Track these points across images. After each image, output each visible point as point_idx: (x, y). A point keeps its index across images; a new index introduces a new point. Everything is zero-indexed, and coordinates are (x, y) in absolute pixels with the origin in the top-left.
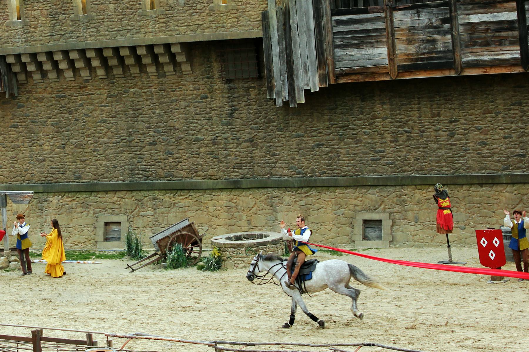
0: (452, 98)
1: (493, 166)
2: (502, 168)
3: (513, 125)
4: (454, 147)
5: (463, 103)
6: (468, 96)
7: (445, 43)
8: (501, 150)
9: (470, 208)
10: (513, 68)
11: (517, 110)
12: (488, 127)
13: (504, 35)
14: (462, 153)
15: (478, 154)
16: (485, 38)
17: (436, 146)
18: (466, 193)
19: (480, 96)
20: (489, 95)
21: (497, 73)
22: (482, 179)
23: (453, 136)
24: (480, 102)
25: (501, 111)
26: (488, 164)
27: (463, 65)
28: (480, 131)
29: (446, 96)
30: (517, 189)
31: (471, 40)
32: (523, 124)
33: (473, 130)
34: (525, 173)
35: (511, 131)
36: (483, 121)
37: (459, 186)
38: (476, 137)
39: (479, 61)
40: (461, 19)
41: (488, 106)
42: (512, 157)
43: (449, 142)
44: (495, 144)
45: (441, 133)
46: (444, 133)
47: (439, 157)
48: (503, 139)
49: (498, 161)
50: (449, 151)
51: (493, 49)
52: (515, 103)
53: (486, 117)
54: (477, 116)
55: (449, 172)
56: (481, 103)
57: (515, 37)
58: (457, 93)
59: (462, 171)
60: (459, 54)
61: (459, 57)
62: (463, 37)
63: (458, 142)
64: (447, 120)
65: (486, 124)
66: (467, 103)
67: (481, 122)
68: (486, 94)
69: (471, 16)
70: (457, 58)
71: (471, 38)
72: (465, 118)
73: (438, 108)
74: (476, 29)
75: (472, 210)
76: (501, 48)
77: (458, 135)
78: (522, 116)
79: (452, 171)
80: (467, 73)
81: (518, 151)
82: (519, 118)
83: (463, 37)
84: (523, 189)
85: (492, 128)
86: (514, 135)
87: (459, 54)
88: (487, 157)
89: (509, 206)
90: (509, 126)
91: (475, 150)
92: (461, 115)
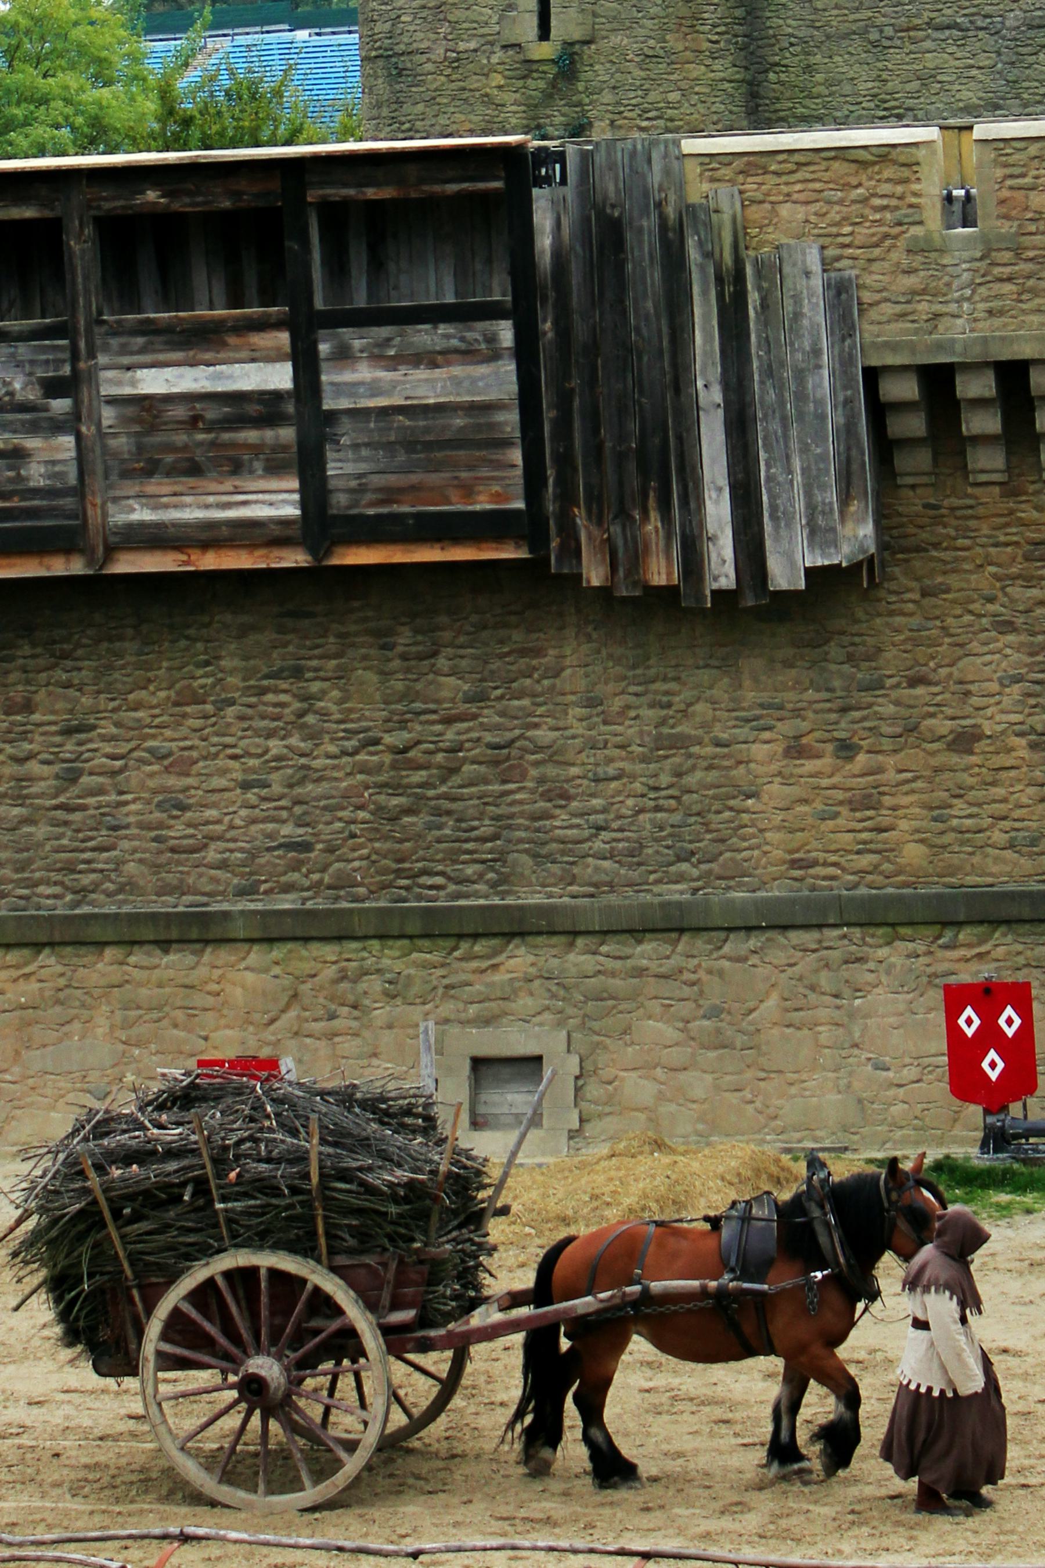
0: (75, 649)
1: (204, 880)
2: (236, 886)
3: (272, 743)
4: (77, 817)
5: (110, 667)
6: (127, 644)
7: (54, 463)
8: (232, 827)
9: (127, 1025)
10: (276, 552)
11: (285, 691)
12: (190, 748)
13: (250, 441)
14: (102, 837)
15: (155, 839)
16: (185, 448)
17: (16, 811)
18: (115, 974)
19: (166, 644)
20: (194, 640)
21: (224, 567)
22: (168, 927)
23: (74, 781)
24: (165, 664)
25: (237, 695)
26: (188, 873)
27: (112, 539)
28: (166, 762)
29: (54, 642)
30: (283, 960)
31: (139, 454)
32: (303, 740)
33: (140, 760)
34: (309, 905)
35: (268, 761)
36: (174, 730)
37: (92, 949)
38: (151, 783)
39: (166, 527)
40: (110, 381)
41: (193, 678)
42: (269, 849)
43: (62, 799)
44: (215, 805)
45: (34, 767)
46: (45, 767)
47: (27, 850)
48: (239, 791)
49: (223, 865)
50: (61, 830)
51: (213, 487)
52: (282, 670)
53: (185, 716)
54: (157, 711)
55: (59, 902)
56: (169, 669)
57: (284, 448)
58: (89, 632)
59: (102, 897)
60: (99, 501)
61: (99, 511)
62: (113, 443)
63: (91, 801)
64: (55, 723)
65: (185, 739)
66: (123, 667)
67: (168, 733)
68: (187, 638)
69: (141, 373)
70: (93, 515)
71: (140, 448)
72: (115, 716)
73: (28, 682)
74: (156, 417)
75: (135, 1031)
76: (237, 483)
77: (91, 774)
78: (301, 714)
79: (69, 897)
80: (127, 564)
81: (287, 830)
82: (292, 718)
83: (113, 443)
84: (301, 959)
85: (204, 753)
86: (275, 776)
87: (99, 501)
88: (184, 852)
89: (256, 1017)
90: (258, 746)
91: (150, 829)
92: (102, 708)
